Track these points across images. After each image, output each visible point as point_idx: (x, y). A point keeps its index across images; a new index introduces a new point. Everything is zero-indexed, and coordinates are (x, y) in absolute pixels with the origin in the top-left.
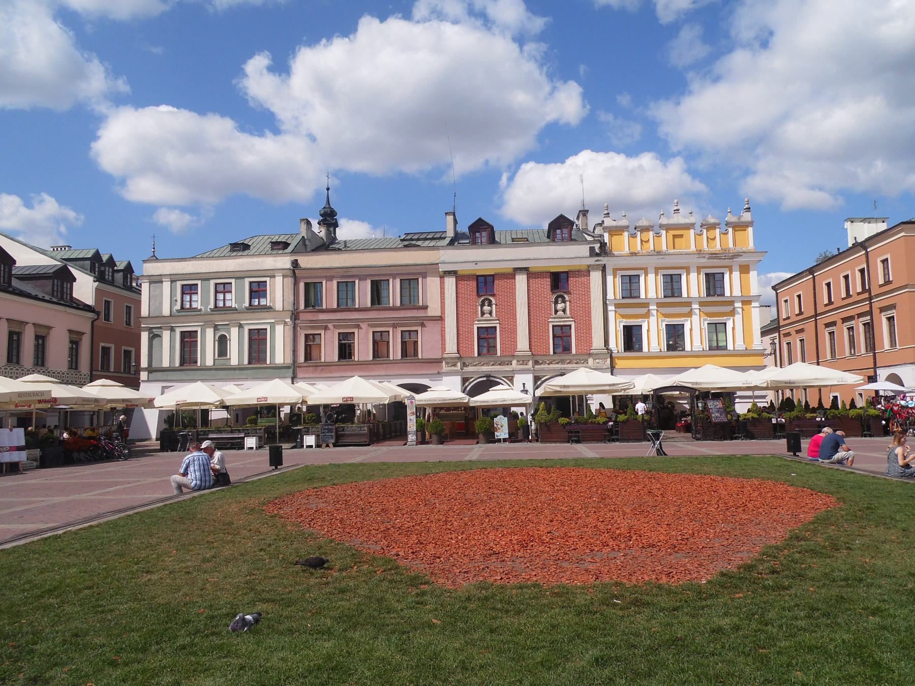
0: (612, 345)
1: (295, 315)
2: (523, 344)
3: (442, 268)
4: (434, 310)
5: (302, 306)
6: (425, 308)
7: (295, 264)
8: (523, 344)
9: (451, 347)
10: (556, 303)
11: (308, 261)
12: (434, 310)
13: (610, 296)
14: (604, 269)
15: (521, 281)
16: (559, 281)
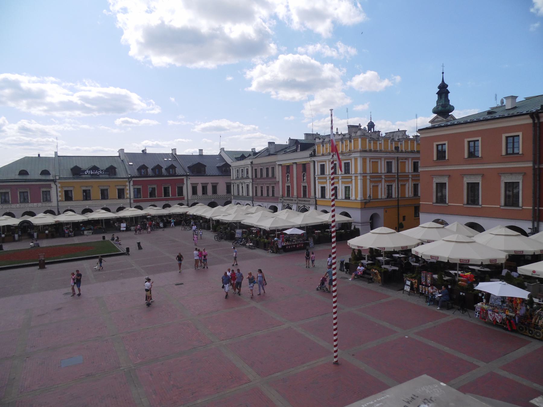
0: (317, 196)
1: (252, 179)
2: (295, 194)
3: (278, 163)
4: (277, 180)
5: (254, 177)
6: (276, 178)
7: (252, 163)
8: (295, 194)
9: (281, 194)
10: (304, 176)
11: (256, 161)
12: (277, 180)
13: (316, 174)
14: (314, 162)
15: (295, 166)
16: (304, 167)
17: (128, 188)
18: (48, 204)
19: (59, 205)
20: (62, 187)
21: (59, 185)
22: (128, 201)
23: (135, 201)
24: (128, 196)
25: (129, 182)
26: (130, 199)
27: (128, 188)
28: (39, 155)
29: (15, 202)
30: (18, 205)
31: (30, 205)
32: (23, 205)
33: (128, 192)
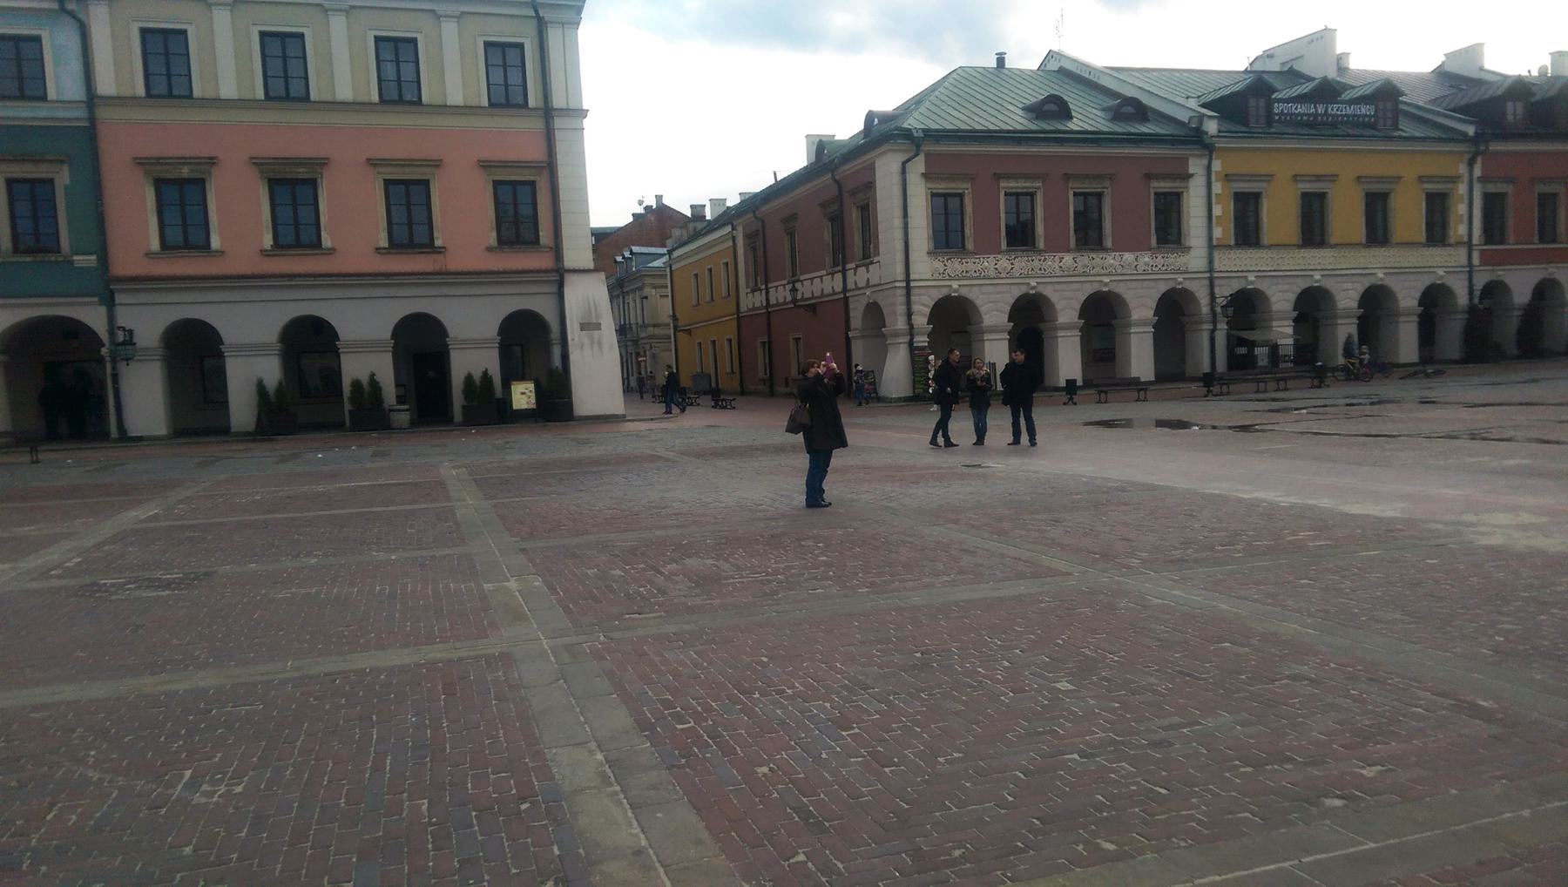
17: (1462, 189)
18: (1175, 260)
19: (1217, 265)
20: (1228, 178)
21: (1217, 166)
22: (1463, 252)
23: (1487, 259)
24: (1462, 229)
25: (1471, 163)
26: (1470, 245)
27: (1462, 189)
28: (1001, 61)
29: (1057, 246)
30: (1068, 259)
31: (1111, 260)
32: (1086, 260)
33: (1462, 209)
